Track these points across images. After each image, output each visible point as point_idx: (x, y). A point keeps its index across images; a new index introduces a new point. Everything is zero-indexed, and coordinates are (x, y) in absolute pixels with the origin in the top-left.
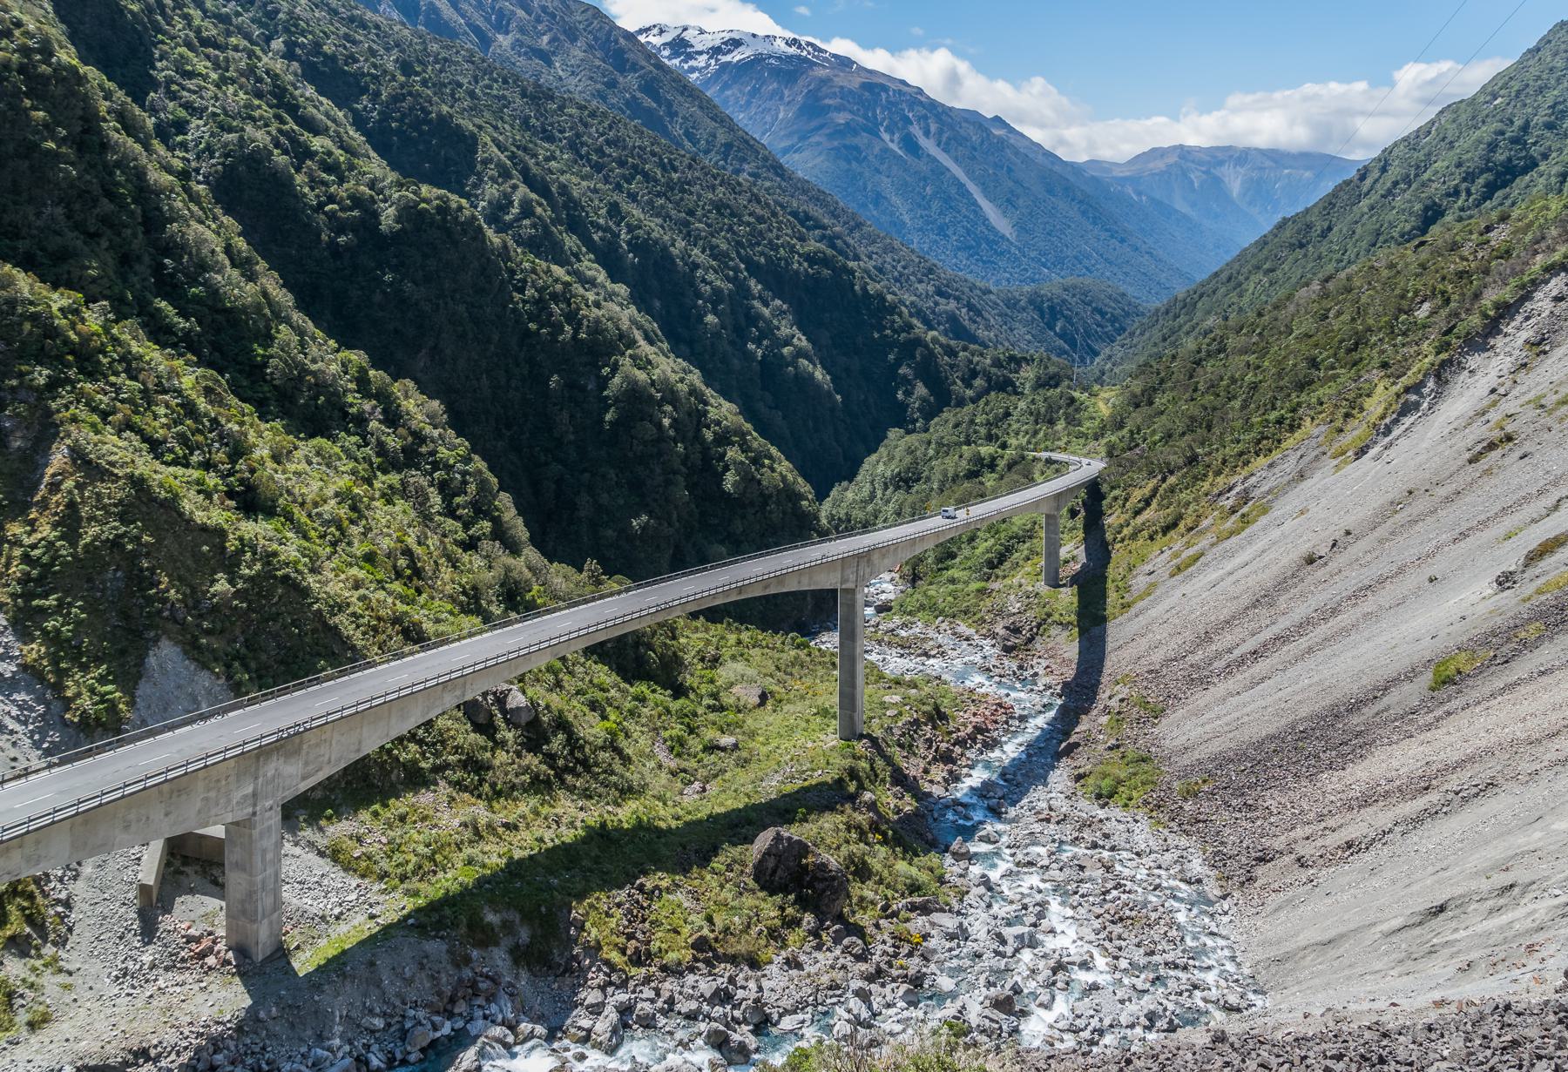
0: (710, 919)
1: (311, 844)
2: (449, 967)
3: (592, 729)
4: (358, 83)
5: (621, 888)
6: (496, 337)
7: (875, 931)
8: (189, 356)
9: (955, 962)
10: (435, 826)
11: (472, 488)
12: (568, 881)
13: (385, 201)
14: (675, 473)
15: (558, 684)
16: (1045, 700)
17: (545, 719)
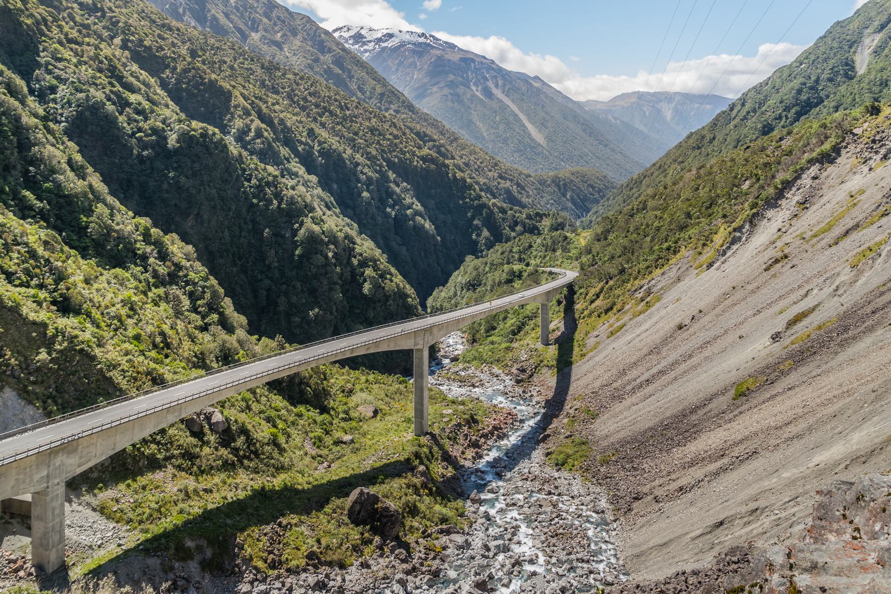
0: (319, 541)
1: (88, 504)
2: (161, 573)
3: (263, 432)
5: (268, 524)
7: (415, 545)
8: (42, 223)
9: (459, 562)
10: (163, 491)
11: (208, 295)
12: (238, 521)
14: (335, 284)
15: (249, 408)
17: (234, 428)
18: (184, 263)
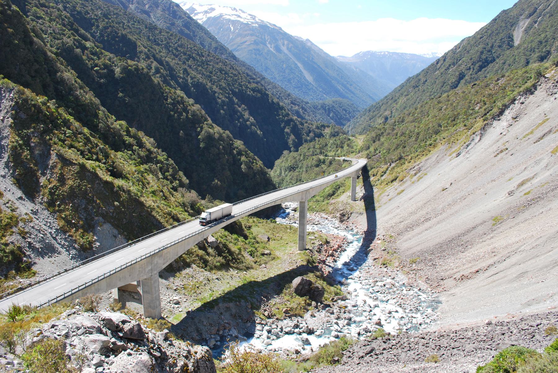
4: (91, 22)
13: (115, 66)
18: (152, 149)
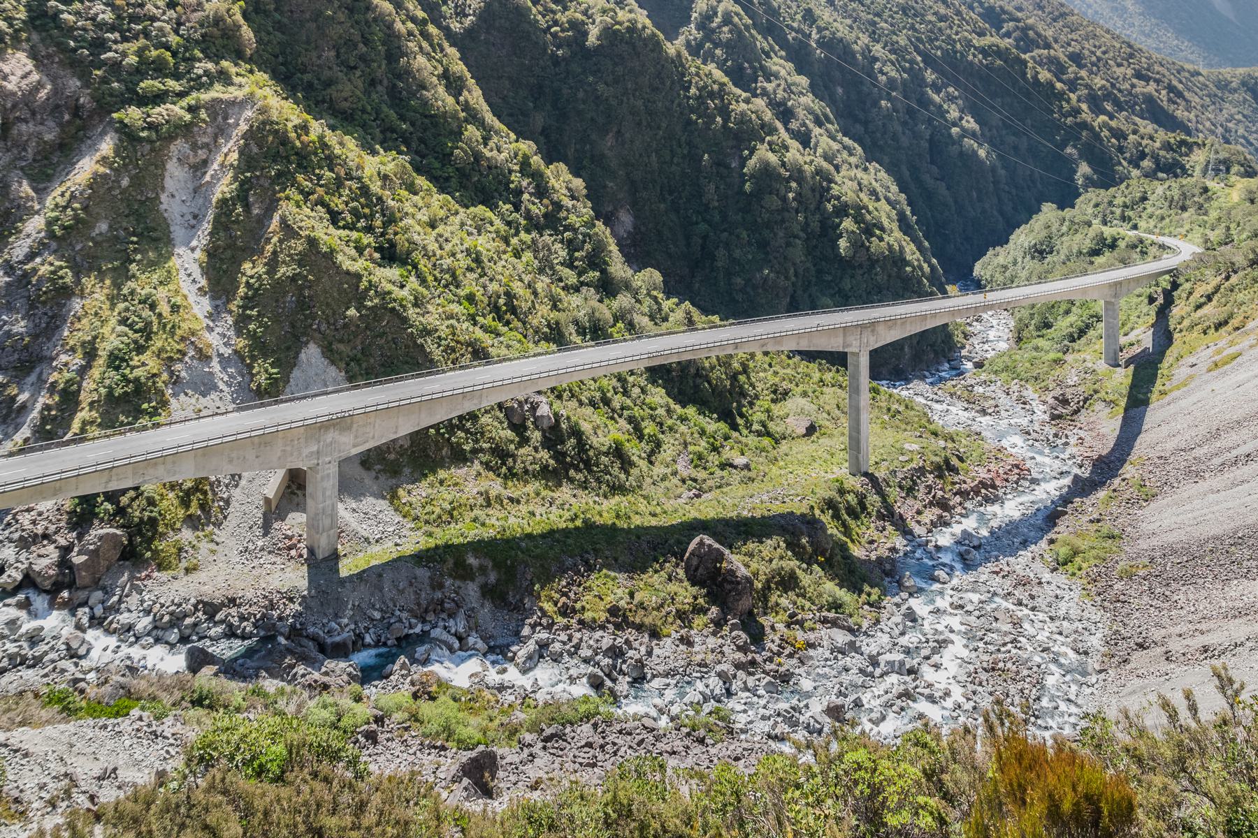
0: (632, 595)
6: (664, 125)
16: (1065, 469)
18: (568, 202)
